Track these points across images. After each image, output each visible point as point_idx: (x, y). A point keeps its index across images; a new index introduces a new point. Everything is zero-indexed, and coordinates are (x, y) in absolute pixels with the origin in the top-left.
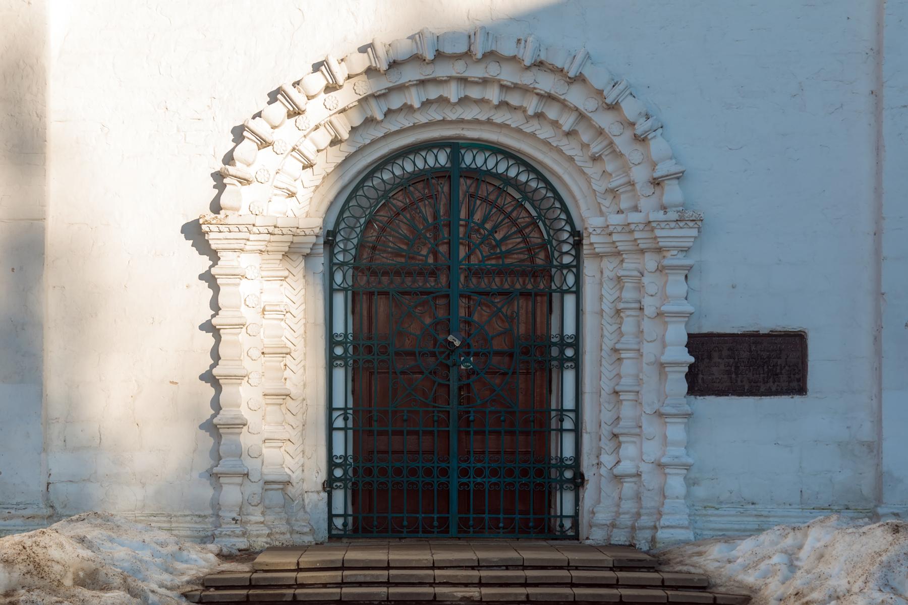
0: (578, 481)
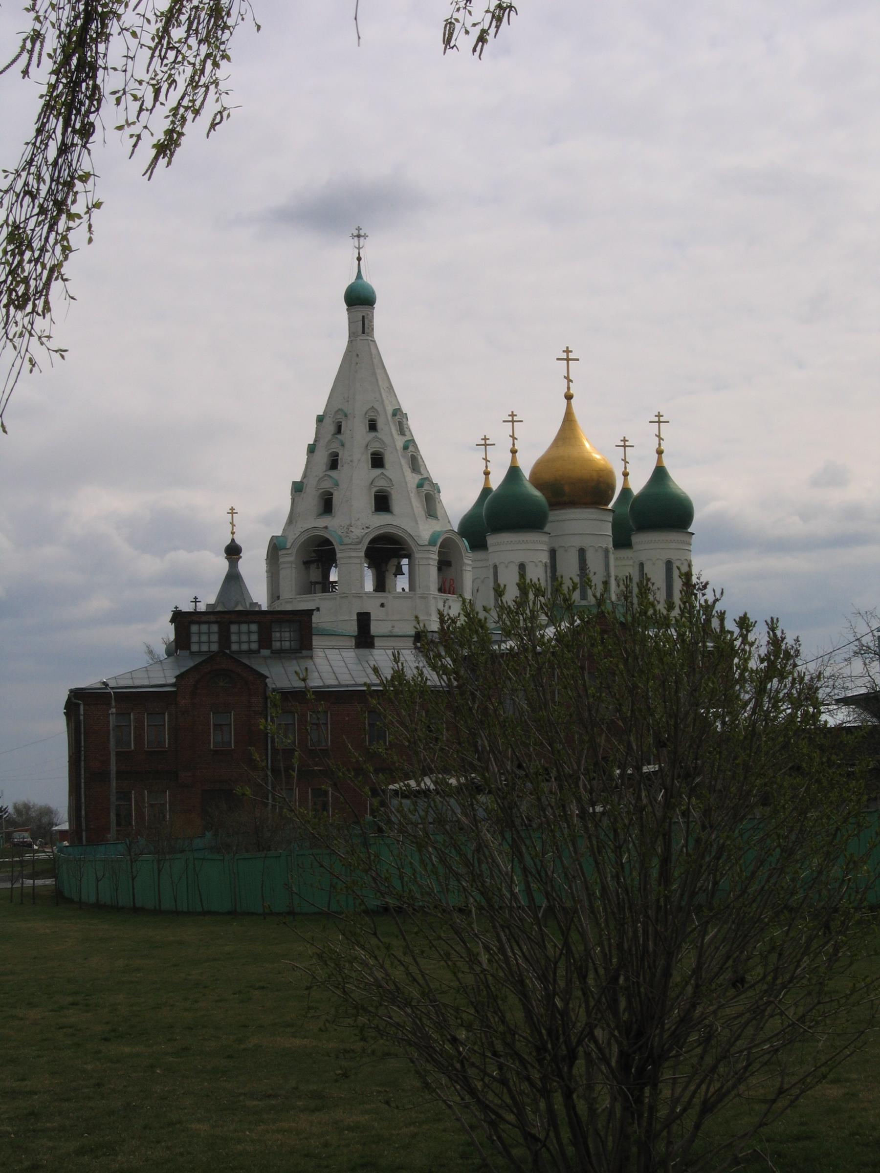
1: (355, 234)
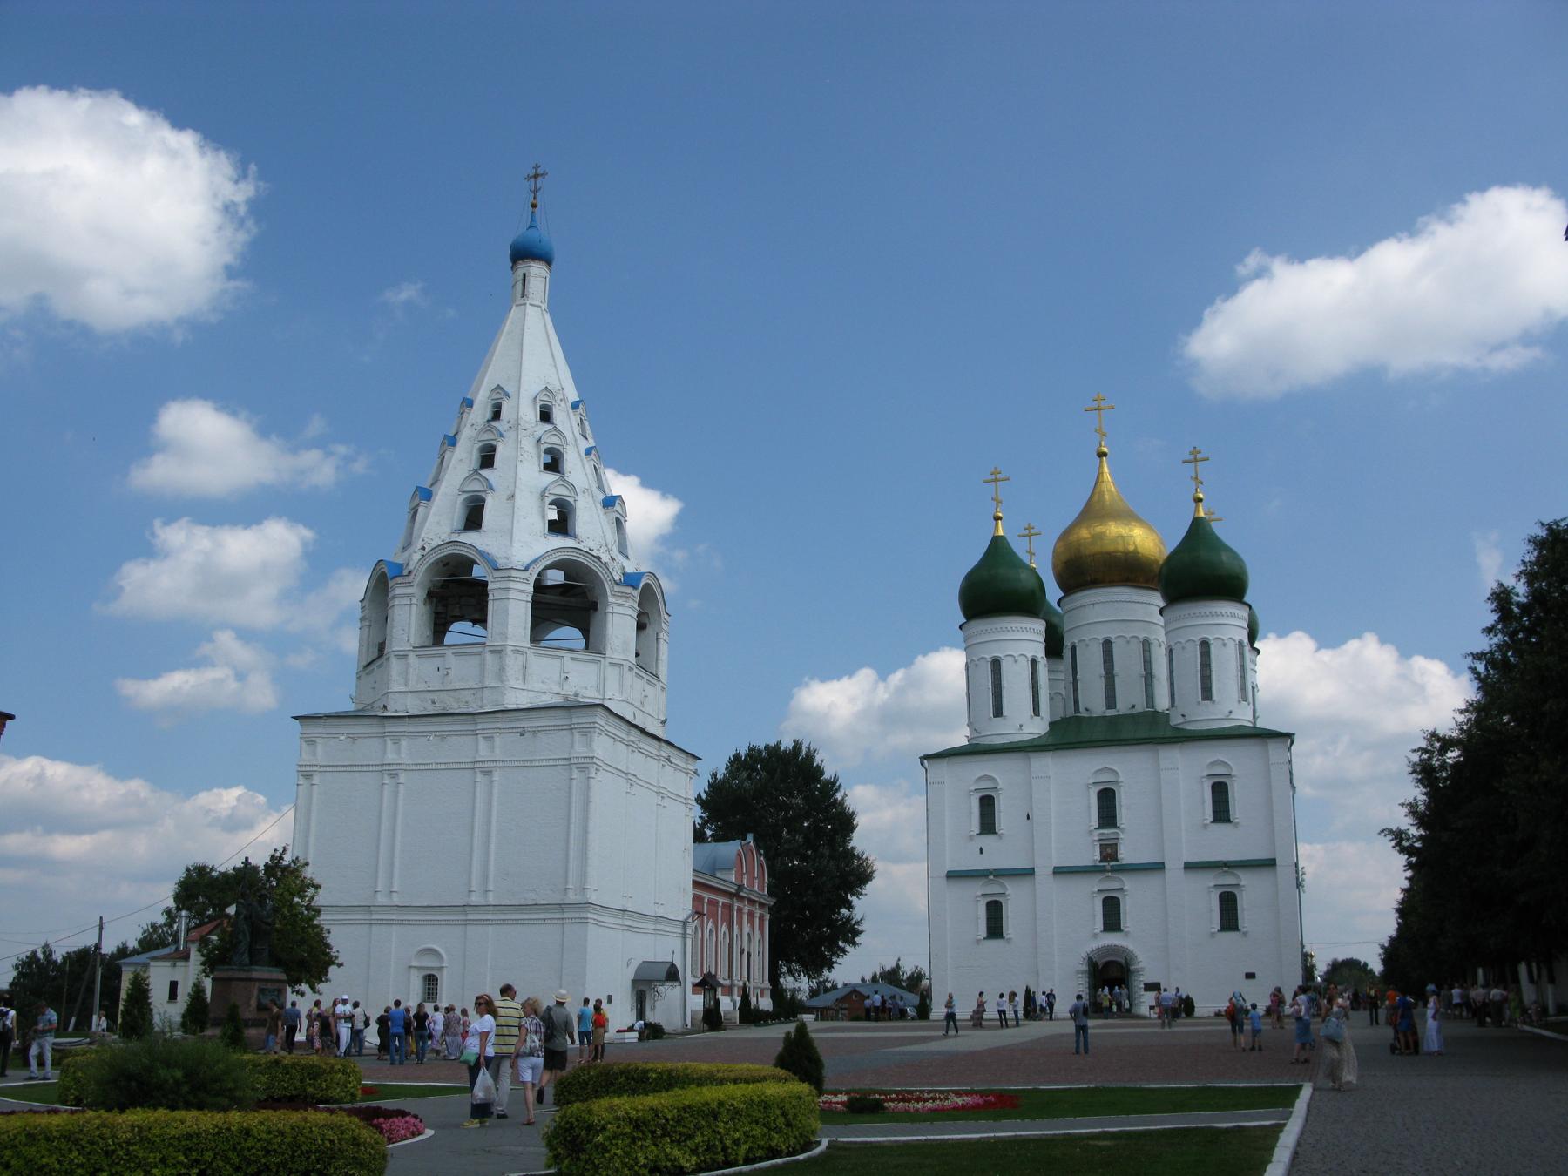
1: (531, 175)
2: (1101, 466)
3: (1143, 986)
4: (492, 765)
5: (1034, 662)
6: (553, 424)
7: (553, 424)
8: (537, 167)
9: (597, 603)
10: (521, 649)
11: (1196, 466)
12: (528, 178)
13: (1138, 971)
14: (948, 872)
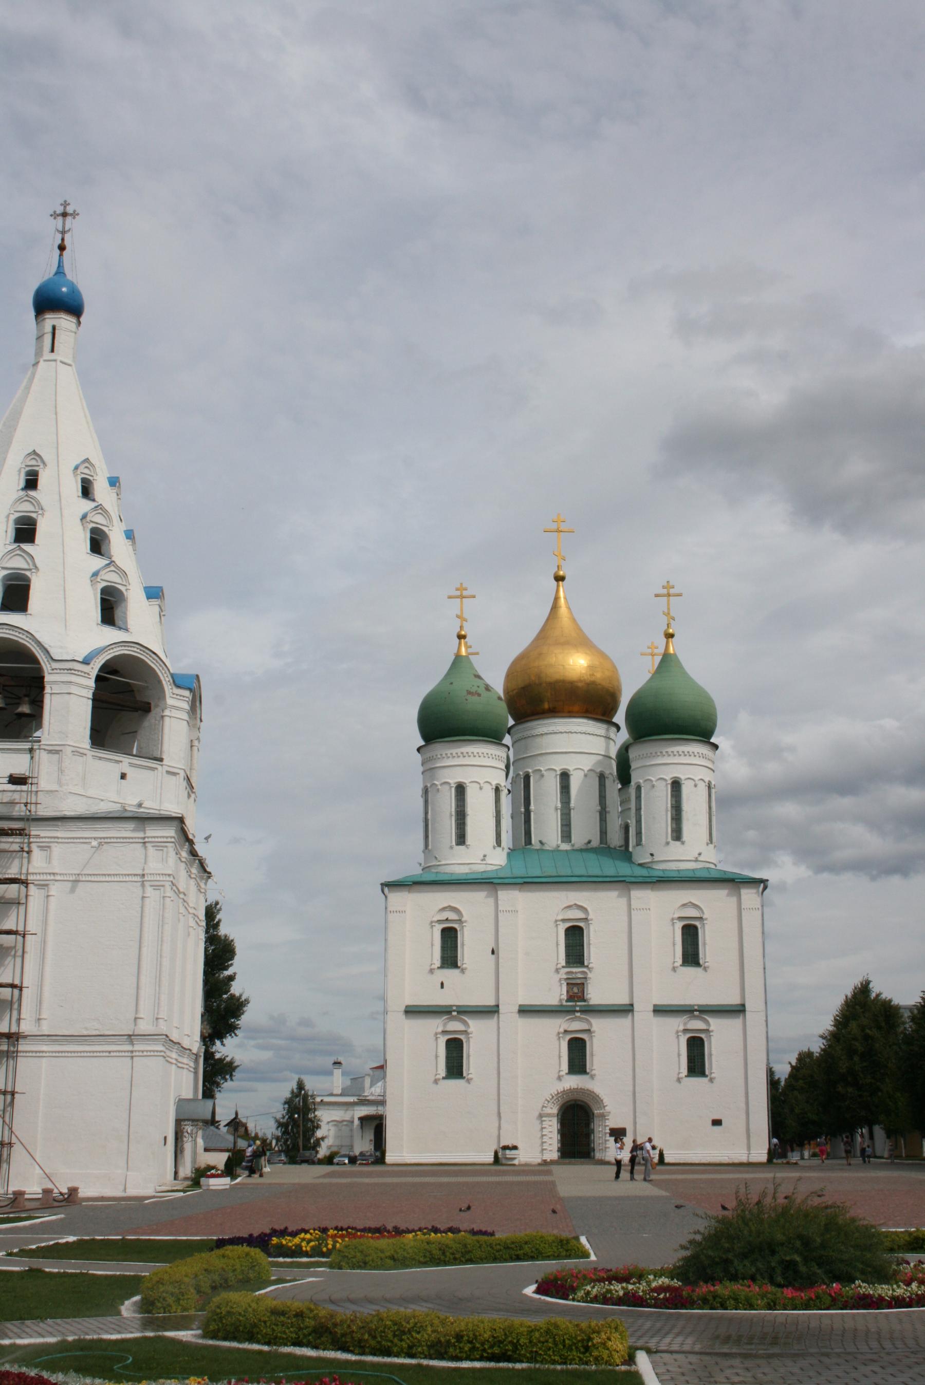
0: (594, 1150)
1: (58, 212)
2: (557, 591)
3: (608, 1131)
4: (49, 877)
5: (497, 790)
6: (94, 500)
7: (94, 500)
8: (65, 204)
9: (149, 704)
10: (82, 751)
11: (668, 601)
12: (55, 215)
13: (603, 1116)
14: (407, 1007)
